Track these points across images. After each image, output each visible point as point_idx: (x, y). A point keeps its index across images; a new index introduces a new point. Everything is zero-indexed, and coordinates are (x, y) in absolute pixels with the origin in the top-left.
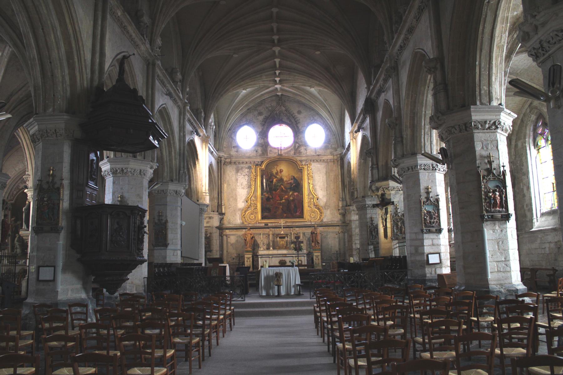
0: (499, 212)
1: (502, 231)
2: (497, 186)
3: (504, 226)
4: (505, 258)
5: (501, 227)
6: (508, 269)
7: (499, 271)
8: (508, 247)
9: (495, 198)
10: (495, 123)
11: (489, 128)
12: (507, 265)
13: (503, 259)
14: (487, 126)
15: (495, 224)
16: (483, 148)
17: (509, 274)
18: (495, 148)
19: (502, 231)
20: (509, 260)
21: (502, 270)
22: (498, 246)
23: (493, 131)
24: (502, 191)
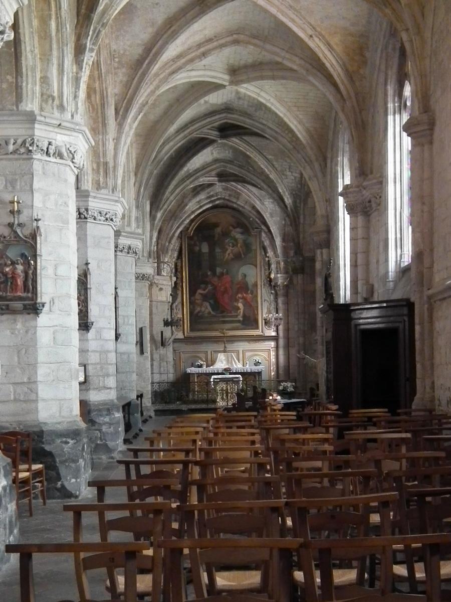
0: (20, 299)
1: (27, 332)
2: (23, 255)
3: (32, 323)
4: (29, 379)
5: (27, 324)
6: (33, 397)
7: (15, 400)
8: (36, 359)
9: (14, 277)
10: (24, 142)
11: (15, 152)
12: (32, 391)
13: (25, 380)
14: (11, 148)
15: (15, 320)
16: (6, 186)
17: (33, 405)
18: (28, 188)
19: (27, 332)
20: (35, 382)
21: (22, 398)
22: (19, 357)
23: (25, 156)
24: (29, 264)
